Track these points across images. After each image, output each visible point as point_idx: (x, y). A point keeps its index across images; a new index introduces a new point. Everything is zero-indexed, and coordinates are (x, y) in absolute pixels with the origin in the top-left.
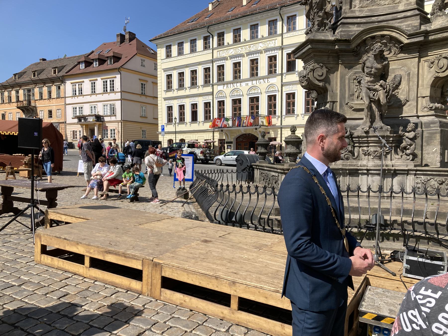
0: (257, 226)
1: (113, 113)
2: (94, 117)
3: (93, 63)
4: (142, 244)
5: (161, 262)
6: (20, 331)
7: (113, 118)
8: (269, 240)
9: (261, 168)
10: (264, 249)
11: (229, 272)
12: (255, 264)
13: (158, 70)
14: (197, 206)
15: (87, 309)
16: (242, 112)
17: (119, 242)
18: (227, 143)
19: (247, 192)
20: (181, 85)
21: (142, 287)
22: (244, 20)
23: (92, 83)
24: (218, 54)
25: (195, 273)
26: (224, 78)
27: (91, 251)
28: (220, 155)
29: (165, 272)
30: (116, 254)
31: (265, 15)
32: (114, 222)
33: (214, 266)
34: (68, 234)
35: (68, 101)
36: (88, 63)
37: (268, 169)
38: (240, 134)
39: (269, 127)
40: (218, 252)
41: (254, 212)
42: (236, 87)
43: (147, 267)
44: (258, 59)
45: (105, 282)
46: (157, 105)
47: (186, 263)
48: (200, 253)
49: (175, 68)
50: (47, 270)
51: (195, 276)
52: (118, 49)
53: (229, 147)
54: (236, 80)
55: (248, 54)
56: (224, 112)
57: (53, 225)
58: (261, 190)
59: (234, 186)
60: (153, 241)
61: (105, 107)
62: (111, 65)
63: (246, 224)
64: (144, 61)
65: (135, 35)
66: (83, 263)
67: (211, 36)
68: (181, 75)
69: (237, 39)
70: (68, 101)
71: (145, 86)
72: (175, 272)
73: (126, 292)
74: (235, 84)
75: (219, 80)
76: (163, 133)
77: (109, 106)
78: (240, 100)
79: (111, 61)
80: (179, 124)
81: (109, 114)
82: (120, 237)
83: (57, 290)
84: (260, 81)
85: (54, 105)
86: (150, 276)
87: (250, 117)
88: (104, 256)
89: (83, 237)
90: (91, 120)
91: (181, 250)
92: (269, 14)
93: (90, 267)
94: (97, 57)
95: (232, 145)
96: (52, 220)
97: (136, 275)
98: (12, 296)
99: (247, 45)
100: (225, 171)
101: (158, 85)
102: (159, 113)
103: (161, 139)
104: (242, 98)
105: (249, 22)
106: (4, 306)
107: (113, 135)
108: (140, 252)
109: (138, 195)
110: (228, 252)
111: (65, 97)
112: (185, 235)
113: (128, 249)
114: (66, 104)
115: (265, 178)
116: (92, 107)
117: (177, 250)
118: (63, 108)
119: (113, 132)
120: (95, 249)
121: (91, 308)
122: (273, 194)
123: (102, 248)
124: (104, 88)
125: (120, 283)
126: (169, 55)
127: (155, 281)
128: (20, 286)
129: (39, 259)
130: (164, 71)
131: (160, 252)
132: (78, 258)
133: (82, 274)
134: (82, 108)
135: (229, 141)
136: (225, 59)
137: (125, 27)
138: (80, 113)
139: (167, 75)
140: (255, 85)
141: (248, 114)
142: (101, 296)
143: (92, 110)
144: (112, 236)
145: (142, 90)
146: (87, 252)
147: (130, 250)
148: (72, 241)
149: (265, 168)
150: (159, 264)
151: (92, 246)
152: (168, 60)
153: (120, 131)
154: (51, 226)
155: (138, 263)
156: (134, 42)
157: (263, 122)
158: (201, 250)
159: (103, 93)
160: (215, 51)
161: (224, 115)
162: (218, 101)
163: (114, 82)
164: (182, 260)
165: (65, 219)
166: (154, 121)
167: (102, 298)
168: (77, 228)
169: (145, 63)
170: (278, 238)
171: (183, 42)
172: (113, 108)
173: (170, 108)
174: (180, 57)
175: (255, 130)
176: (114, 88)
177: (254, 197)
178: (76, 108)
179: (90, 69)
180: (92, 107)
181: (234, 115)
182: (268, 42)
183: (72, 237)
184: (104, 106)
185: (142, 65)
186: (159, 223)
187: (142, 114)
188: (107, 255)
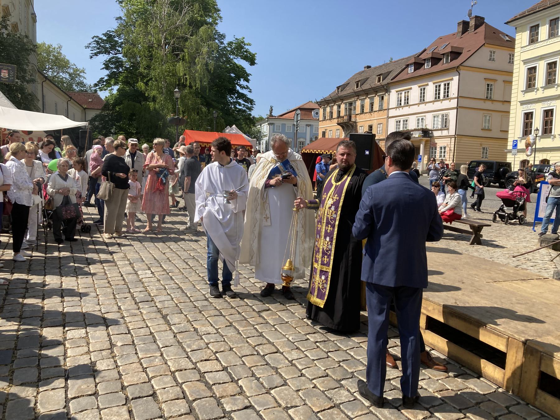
1: (445, 126)
2: (421, 132)
3: (424, 64)
6: (347, 393)
7: (445, 133)
13: (515, 63)
15: (425, 387)
23: (421, 89)
27: (430, 308)
32: (456, 271)
35: (392, 113)
36: (418, 65)
43: (515, 350)
46: (509, 112)
52: (457, 43)
61: (436, 119)
62: (447, 65)
64: (494, 52)
65: (483, 19)
70: (392, 113)
71: (493, 87)
76: (514, 151)
77: (440, 117)
79: (447, 59)
80: (541, 137)
81: (440, 127)
82: (468, 296)
90: (417, 136)
94: (430, 56)
98: (336, 344)
101: (514, 83)
102: (510, 124)
103: (510, 159)
107: (443, 154)
109: (481, 236)
111: (388, 109)
114: (389, 117)
116: (418, 120)
118: (384, 121)
119: (443, 150)
120: (436, 306)
121: (429, 387)
124: (436, 94)
126: (533, 40)
130: (525, 63)
134: (407, 121)
137: (470, 10)
138: (403, 127)
139: (529, 69)
143: (418, 123)
145: (487, 93)
152: (533, 46)
153: (453, 149)
156: (482, 29)
159: (434, 101)
163: (450, 86)
166: (501, 135)
169: (495, 56)
172: (446, 119)
173: (528, 116)
174: (552, 40)
176: (450, 94)
178: (400, 122)
179: (420, 72)
180: (418, 120)
184: (434, 117)
185: (490, 59)
186: (525, 284)
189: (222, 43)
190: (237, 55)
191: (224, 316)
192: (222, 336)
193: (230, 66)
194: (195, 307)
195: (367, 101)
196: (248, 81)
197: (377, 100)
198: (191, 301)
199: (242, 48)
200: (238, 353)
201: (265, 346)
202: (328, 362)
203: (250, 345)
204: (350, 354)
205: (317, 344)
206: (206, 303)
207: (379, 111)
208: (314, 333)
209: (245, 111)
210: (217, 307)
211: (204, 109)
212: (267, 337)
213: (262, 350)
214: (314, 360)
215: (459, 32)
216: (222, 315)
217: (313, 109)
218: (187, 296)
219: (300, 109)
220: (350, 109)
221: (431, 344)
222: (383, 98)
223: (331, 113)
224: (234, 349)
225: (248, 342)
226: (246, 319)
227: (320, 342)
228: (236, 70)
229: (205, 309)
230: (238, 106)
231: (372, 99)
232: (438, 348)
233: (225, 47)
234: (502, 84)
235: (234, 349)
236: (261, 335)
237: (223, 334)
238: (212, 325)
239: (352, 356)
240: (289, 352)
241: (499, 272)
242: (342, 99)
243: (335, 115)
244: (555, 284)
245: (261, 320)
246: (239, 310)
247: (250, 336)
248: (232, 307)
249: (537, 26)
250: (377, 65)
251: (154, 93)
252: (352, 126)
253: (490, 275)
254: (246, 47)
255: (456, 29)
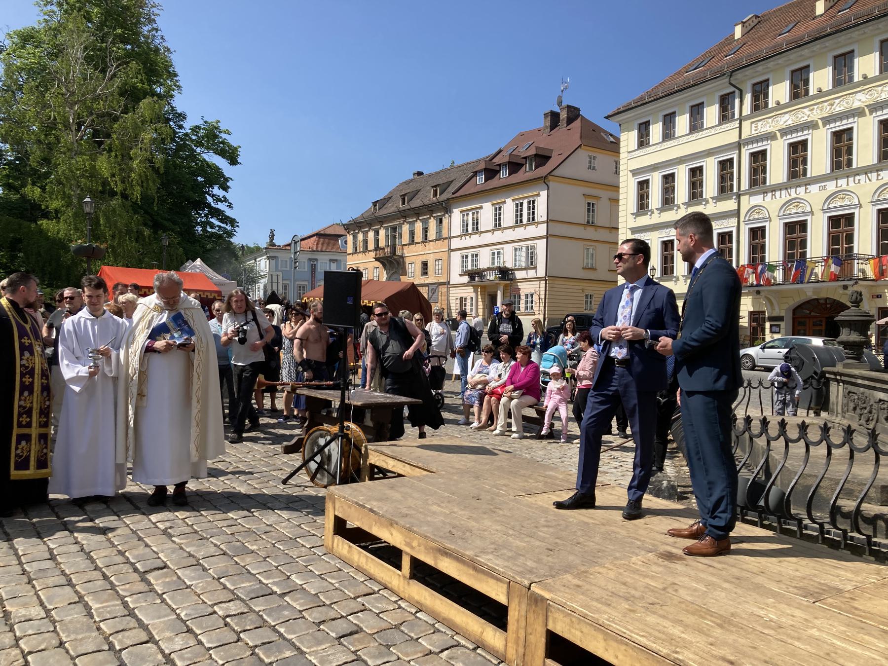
0: (827, 526)
1: (532, 264)
3: (498, 172)
4: (518, 543)
5: (547, 595)
8: (849, 575)
9: (847, 379)
10: (830, 600)
11: (712, 655)
12: (797, 643)
13: (621, 174)
14: (680, 460)
16: (808, 250)
17: (471, 531)
18: (771, 319)
19: (798, 440)
20: (668, 201)
21: (506, 646)
22: (817, 46)
23: (496, 209)
24: (754, 128)
25: (621, 639)
26: (765, 179)
27: (415, 544)
28: (752, 345)
29: (554, 622)
30: (458, 558)
31: (870, 28)
33: (676, 631)
34: (380, 500)
35: (455, 243)
36: (491, 173)
37: (866, 383)
38: (803, 298)
39: (879, 283)
40: (696, 590)
41: (821, 491)
42: (794, 195)
43: (516, 601)
44: (851, 129)
45: (437, 617)
47: (604, 608)
48: (647, 587)
49: (654, 168)
50: (340, 570)
51: (623, 647)
52: (544, 142)
53: (774, 329)
54: (795, 181)
55: (827, 121)
56: (763, 251)
57: (376, 476)
58: (836, 437)
59: (765, 422)
60: (543, 540)
63: (792, 517)
64: (594, 158)
65: (578, 110)
66: (399, 567)
67: (737, 92)
68: (669, 179)
69: (799, 91)
70: (455, 243)
72: (577, 627)
73: (475, 649)
74: (793, 190)
75: (754, 183)
77: (524, 249)
78: (803, 225)
79: (531, 165)
80: (661, 279)
83: (342, 617)
84: (857, 178)
85: (431, 252)
86: (523, 624)
87: (831, 261)
88: (435, 559)
89: (405, 511)
91: (601, 570)
92: (880, 26)
93: (410, 578)
94: (507, 159)
95: (782, 324)
96: (373, 466)
97: (494, 613)
98: (261, 616)
99: (823, 102)
100: (755, 384)
101: (621, 203)
104: (809, 218)
105: (831, 50)
106: (242, 635)
108: (506, 564)
110: (723, 594)
111: (450, 238)
112: (624, 533)
113: (484, 551)
114: (451, 250)
115: (860, 407)
117: (592, 570)
118: (444, 256)
120: (422, 540)
122: (871, 450)
123: (434, 541)
125: (464, 625)
126: (643, 142)
127: (532, 638)
128: (284, 594)
129: (330, 543)
130: (634, 175)
131: (551, 568)
132: (391, 555)
133: (396, 589)
134: (477, 255)
135: (775, 315)
136: (771, 137)
137: (560, 98)
138: (472, 265)
140: (844, 187)
141: (825, 255)
142: (419, 649)
144: (462, 515)
146: (408, 544)
147: (488, 553)
148: (383, 516)
149: (860, 381)
150: (543, 599)
151: (415, 532)
154: (372, 478)
155: (500, 590)
156: (577, 123)
157: (863, 271)
158: (652, 577)
160: (746, 124)
161: (763, 258)
162: (751, 229)
164: (597, 600)
165: (393, 466)
167: (420, 655)
168: (402, 489)
169: (596, 163)
170: (878, 574)
171: (674, 113)
174: (668, 143)
175: (841, 291)
177: (821, 451)
178: (467, 256)
179: (494, 183)
181: (789, 257)
182: (880, 89)
183: (385, 509)
184: (516, 250)
185: (590, 168)
187: (587, 264)
188: (441, 558)
189: (181, 127)
190: (208, 148)
191: (73, 586)
192: (54, 622)
193: (197, 164)
194: (24, 572)
195: (419, 226)
196: (225, 188)
197: (432, 224)
198: (21, 564)
199: (216, 136)
200: (72, 652)
201: (126, 634)
202: (236, 651)
203: (104, 633)
204: (278, 632)
205: (228, 620)
206: (48, 564)
207: (436, 240)
208: (230, 601)
209: (220, 236)
210: (67, 572)
211: (147, 232)
212: (140, 617)
213: (120, 642)
214: (211, 648)
215: (545, 127)
216: (70, 584)
217: (341, 236)
218: (16, 554)
219: (319, 235)
220: (394, 237)
221: (417, 602)
222: (441, 221)
223: (365, 242)
224: (66, 645)
225: (99, 629)
226: (113, 587)
227: (234, 615)
228: (206, 172)
229: (41, 575)
230: (209, 230)
231: (425, 222)
232: (426, 607)
233: (186, 135)
234: (608, 202)
235: (66, 645)
236: (131, 614)
237: (57, 618)
238: (42, 604)
239: (281, 635)
240: (170, 639)
241: (541, 479)
242: (381, 221)
243: (371, 246)
244: (614, 492)
245: (142, 587)
246: (107, 573)
247: (108, 616)
248: (97, 568)
249: (647, 124)
250: (433, 171)
251: (55, 204)
252: (398, 263)
253: (526, 484)
254: (224, 136)
255: (542, 123)
